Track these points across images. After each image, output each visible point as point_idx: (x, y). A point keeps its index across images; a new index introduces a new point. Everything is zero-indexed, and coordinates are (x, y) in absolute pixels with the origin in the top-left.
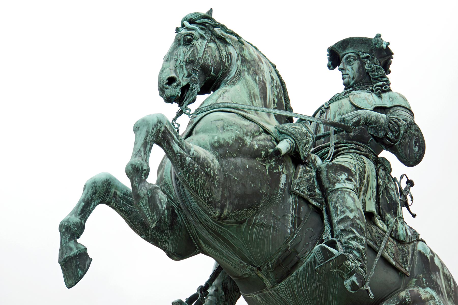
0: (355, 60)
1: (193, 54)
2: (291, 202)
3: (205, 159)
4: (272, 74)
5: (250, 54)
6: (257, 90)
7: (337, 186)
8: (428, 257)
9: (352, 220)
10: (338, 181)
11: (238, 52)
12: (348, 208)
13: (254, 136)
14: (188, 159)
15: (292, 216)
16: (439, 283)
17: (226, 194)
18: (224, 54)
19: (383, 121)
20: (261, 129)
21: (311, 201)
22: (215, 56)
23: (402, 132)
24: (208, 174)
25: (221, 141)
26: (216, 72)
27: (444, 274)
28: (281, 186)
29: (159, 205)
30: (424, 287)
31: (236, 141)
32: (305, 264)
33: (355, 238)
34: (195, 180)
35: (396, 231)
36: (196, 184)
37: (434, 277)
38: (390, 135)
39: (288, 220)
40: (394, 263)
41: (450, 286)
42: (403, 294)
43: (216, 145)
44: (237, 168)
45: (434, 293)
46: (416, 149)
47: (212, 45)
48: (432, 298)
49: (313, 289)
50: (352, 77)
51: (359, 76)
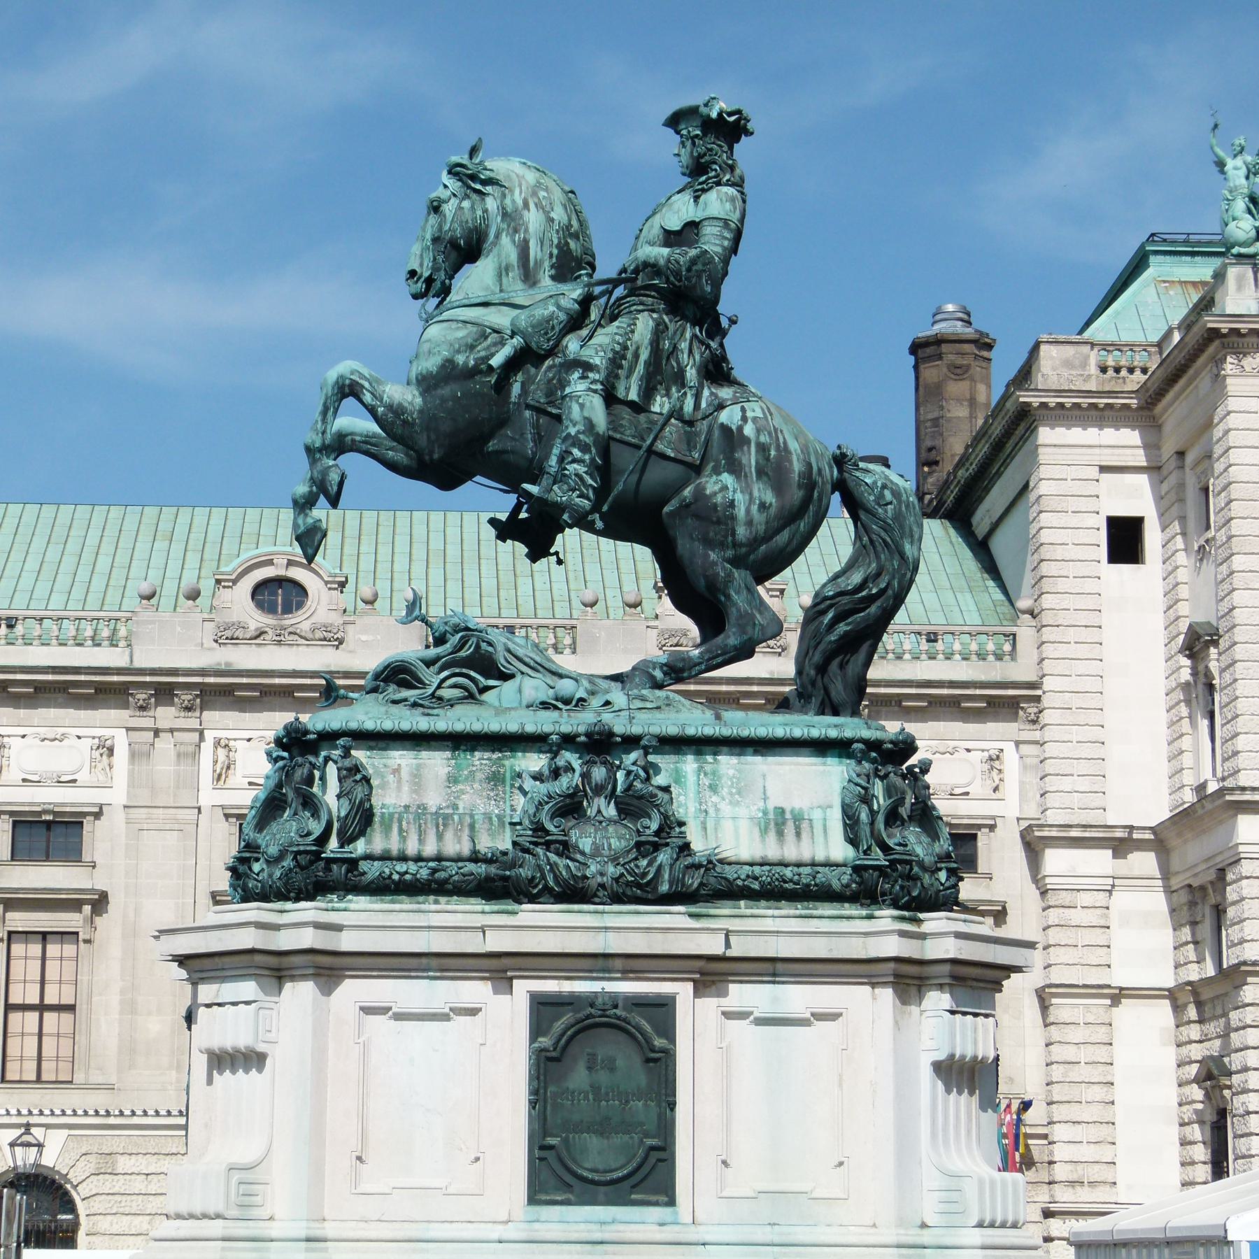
3: (400, 405)
4: (552, 215)
5: (513, 201)
6: (513, 256)
8: (734, 428)
13: (472, 347)
14: (381, 410)
16: (744, 461)
17: (433, 437)
18: (479, 213)
19: (662, 262)
20: (489, 331)
21: (549, 409)
24: (405, 422)
25: (424, 372)
26: (468, 243)
28: (513, 400)
30: (719, 474)
31: (443, 366)
33: (574, 461)
35: (681, 408)
39: (526, 440)
41: (768, 459)
42: (687, 492)
44: (444, 400)
46: (708, 289)
47: (466, 204)
48: (725, 488)
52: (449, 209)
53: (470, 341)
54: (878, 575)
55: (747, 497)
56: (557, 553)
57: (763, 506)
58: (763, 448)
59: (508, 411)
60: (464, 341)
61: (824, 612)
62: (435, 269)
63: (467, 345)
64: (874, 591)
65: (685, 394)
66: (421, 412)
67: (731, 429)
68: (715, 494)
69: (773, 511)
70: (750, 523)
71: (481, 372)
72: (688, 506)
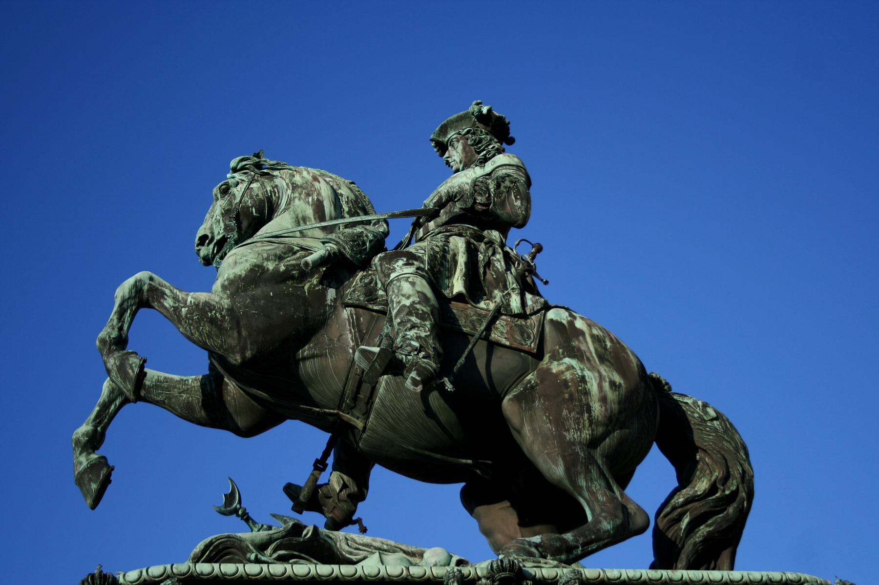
0: (458, 141)
1: (230, 203)
2: (346, 316)
7: (393, 276)
8: (565, 322)
9: (409, 307)
10: (394, 270)
11: (288, 181)
12: (403, 295)
13: (280, 258)
15: (351, 332)
16: (583, 347)
21: (370, 306)
22: (257, 195)
23: (492, 190)
27: (593, 336)
28: (329, 302)
29: (130, 371)
32: (384, 383)
33: (413, 327)
34: (198, 331)
35: (509, 305)
36: (200, 335)
37: (575, 343)
38: (479, 199)
39: (347, 339)
40: (508, 343)
41: (605, 348)
43: (226, 283)
44: (254, 299)
45: (574, 362)
47: (254, 186)
48: (570, 368)
49: (408, 410)
50: (458, 161)
51: (466, 157)
52: (238, 191)
53: (278, 252)
54: (727, 478)
55: (597, 375)
56: (359, 521)
57: (613, 384)
58: (596, 339)
59: (325, 312)
60: (273, 252)
61: (679, 519)
62: (227, 228)
63: (275, 255)
64: (727, 492)
65: (509, 294)
66: (231, 311)
67: (561, 324)
68: (563, 372)
69: (623, 391)
70: (603, 399)
71: (292, 278)
72: (532, 387)
